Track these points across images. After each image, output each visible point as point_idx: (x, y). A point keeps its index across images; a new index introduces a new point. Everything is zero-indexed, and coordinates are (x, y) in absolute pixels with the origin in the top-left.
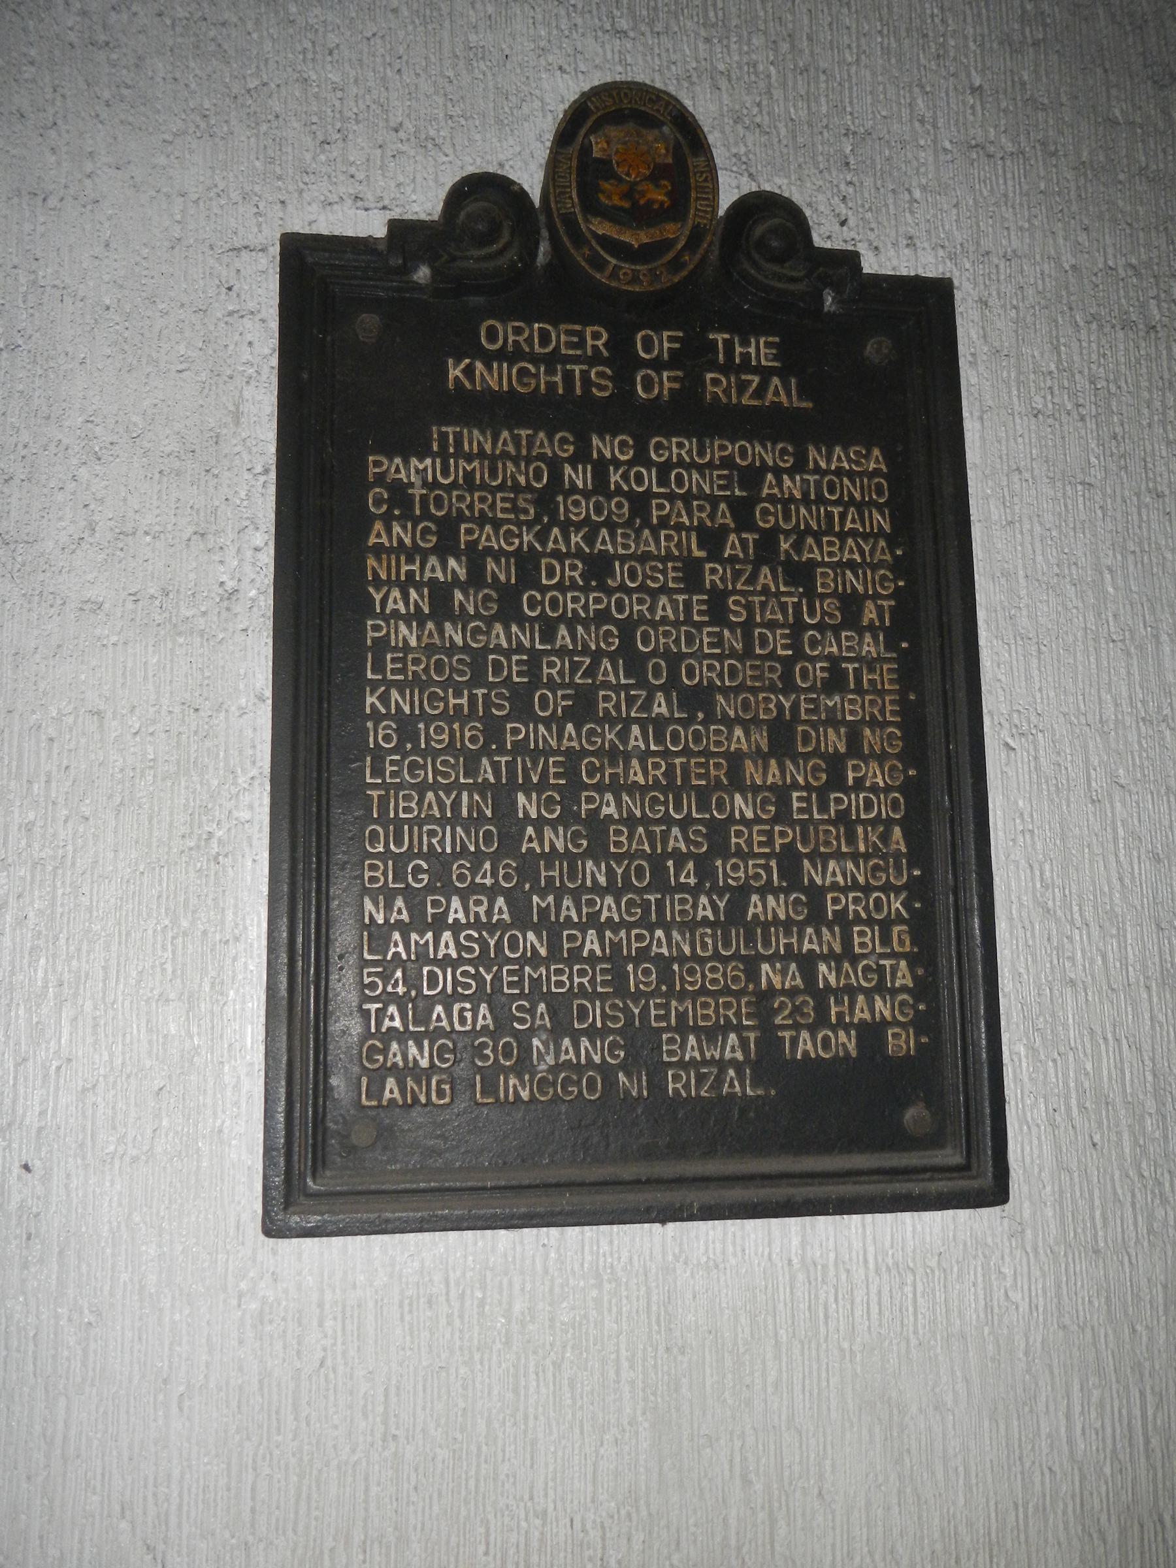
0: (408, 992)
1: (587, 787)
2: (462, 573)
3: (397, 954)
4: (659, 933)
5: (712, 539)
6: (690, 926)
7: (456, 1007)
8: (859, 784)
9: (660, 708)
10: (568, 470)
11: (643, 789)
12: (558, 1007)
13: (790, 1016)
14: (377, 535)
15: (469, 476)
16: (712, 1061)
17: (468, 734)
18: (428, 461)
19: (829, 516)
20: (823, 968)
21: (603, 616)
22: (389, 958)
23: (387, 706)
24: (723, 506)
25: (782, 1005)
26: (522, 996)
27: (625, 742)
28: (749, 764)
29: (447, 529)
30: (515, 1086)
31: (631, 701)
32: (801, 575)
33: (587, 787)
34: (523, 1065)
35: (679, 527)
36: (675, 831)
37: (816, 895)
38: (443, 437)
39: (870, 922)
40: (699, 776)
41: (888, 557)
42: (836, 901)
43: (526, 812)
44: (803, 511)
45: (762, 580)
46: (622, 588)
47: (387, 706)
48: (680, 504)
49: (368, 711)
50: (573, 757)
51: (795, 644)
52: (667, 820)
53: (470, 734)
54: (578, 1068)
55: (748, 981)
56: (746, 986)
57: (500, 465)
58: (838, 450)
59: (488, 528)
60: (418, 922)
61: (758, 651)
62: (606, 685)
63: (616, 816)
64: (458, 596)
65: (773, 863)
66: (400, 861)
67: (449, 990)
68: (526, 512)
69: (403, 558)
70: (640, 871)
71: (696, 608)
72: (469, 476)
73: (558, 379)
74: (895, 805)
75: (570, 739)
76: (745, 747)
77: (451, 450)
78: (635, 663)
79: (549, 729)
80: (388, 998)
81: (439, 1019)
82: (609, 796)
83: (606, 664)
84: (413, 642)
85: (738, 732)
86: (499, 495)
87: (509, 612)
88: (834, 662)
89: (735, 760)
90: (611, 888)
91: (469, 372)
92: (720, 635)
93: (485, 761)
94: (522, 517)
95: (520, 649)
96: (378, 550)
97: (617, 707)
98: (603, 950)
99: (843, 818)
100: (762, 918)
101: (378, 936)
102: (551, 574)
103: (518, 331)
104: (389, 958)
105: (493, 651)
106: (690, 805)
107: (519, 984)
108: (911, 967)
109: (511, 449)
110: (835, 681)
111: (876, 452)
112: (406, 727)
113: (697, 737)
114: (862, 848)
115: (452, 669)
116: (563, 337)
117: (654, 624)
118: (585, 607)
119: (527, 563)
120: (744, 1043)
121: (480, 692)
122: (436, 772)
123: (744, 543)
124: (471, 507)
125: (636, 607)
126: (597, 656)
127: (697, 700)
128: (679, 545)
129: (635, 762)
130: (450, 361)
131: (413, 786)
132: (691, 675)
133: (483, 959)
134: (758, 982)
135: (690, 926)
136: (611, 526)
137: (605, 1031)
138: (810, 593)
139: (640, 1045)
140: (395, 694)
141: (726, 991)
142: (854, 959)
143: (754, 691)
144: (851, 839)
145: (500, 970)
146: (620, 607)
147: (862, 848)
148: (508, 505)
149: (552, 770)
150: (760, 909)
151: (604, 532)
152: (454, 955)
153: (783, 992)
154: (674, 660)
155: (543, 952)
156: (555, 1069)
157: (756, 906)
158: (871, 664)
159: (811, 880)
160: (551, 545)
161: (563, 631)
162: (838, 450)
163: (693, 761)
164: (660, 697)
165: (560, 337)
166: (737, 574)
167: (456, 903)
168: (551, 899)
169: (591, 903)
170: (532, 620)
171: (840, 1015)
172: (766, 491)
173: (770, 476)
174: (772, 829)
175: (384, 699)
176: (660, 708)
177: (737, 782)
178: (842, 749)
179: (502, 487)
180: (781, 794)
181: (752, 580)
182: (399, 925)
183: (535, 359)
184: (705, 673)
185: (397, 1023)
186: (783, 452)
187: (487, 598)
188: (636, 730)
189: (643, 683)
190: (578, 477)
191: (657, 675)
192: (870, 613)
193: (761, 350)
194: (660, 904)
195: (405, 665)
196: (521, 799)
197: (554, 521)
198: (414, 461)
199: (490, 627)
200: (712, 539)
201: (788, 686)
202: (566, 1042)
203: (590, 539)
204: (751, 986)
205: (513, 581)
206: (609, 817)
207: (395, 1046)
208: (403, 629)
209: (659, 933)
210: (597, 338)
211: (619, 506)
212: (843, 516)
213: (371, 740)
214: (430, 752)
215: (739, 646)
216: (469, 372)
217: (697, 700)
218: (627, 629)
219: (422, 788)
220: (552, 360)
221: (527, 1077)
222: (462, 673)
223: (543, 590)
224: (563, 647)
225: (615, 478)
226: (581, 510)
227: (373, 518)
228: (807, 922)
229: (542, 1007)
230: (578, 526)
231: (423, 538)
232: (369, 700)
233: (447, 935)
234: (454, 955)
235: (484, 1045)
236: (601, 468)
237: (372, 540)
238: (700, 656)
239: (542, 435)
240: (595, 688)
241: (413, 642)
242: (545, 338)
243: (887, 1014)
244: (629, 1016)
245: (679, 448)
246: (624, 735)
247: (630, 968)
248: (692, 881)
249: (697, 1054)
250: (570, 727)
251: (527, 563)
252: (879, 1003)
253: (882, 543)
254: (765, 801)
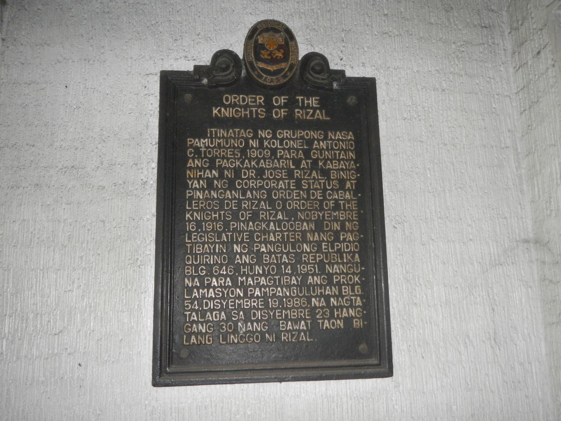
0: (199, 308)
2: (217, 175)
4: (279, 289)
5: (297, 163)
7: (214, 313)
8: (344, 240)
9: (280, 216)
10: (251, 141)
11: (274, 243)
12: (247, 312)
13: (322, 315)
14: (190, 164)
17: (218, 226)
18: (206, 140)
19: (335, 154)
20: (332, 300)
21: (262, 187)
23: (193, 217)
24: (300, 152)
25: (319, 312)
26: (235, 309)
27: (269, 228)
29: (212, 161)
32: (326, 173)
33: (256, 242)
34: (235, 331)
35: (286, 159)
36: (285, 256)
37: (330, 276)
38: (211, 132)
39: (348, 285)
40: (292, 238)
41: (354, 167)
44: (326, 152)
45: (313, 175)
46: (268, 178)
47: (193, 217)
48: (286, 151)
49: (187, 219)
50: (252, 233)
53: (219, 226)
58: (338, 133)
59: (225, 161)
60: (202, 286)
61: (312, 198)
62: (263, 210)
65: (316, 266)
66: (197, 267)
67: (212, 307)
68: (237, 155)
69: (198, 171)
71: (292, 184)
73: (248, 113)
75: (251, 227)
79: (244, 224)
80: (192, 310)
82: (263, 245)
83: (263, 203)
85: (305, 224)
86: (229, 150)
87: (231, 186)
88: (336, 201)
89: (304, 233)
90: (264, 275)
91: (220, 111)
92: (299, 193)
93: (224, 234)
95: (235, 198)
96: (190, 168)
97: (266, 216)
98: (261, 294)
99: (339, 251)
101: (190, 291)
102: (245, 174)
103: (235, 98)
105: (226, 199)
106: (289, 248)
107: (234, 305)
108: (361, 299)
109: (233, 135)
110: (337, 207)
111: (351, 133)
112: (199, 224)
114: (345, 261)
115: (213, 205)
116: (250, 100)
118: (256, 185)
120: (306, 324)
121: (222, 212)
123: (307, 163)
124: (220, 154)
126: (260, 200)
127: (292, 214)
128: (286, 164)
129: (272, 234)
130: (214, 108)
131: (201, 243)
132: (290, 206)
133: (223, 298)
135: (289, 286)
138: (329, 179)
140: (195, 214)
141: (301, 307)
142: (343, 297)
143: (310, 211)
144: (342, 258)
146: (267, 185)
147: (345, 261)
149: (245, 237)
150: (312, 281)
151: (262, 161)
152: (214, 296)
153: (319, 307)
154: (284, 201)
155: (242, 295)
159: (329, 271)
160: (245, 165)
161: (249, 193)
162: (338, 133)
163: (290, 234)
164: (280, 213)
165: (249, 99)
167: (214, 280)
168: (244, 278)
169: (257, 279)
171: (338, 315)
172: (314, 147)
173: (316, 142)
174: (316, 255)
175: (192, 215)
176: (280, 216)
177: (304, 240)
178: (339, 229)
179: (230, 147)
180: (319, 244)
181: (310, 175)
182: (196, 287)
183: (241, 107)
184: (294, 205)
185: (196, 318)
186: (320, 134)
188: (272, 224)
190: (254, 143)
191: (279, 206)
192: (348, 185)
193: (313, 101)
194: (280, 279)
196: (235, 246)
197: (246, 158)
198: (202, 140)
200: (297, 163)
201: (322, 209)
202: (249, 324)
203: (258, 163)
207: (194, 325)
208: (198, 193)
209: (279, 289)
210: (260, 99)
211: (267, 152)
212: (340, 154)
215: (305, 196)
216: (220, 111)
217: (292, 214)
219: (204, 243)
220: (246, 107)
222: (216, 207)
223: (243, 180)
224: (249, 198)
225: (266, 143)
226: (255, 154)
229: (241, 313)
230: (254, 159)
231: (205, 164)
232: (187, 216)
233: (211, 290)
234: (214, 296)
235: (223, 325)
237: (189, 165)
238: (293, 200)
239: (242, 130)
240: (259, 210)
241: (201, 197)
242: (244, 100)
243: (353, 314)
245: (286, 133)
246: (268, 225)
247: (270, 300)
248: (290, 272)
250: (251, 223)
251: (237, 172)
252: (350, 311)
253: (352, 162)
254: (314, 246)
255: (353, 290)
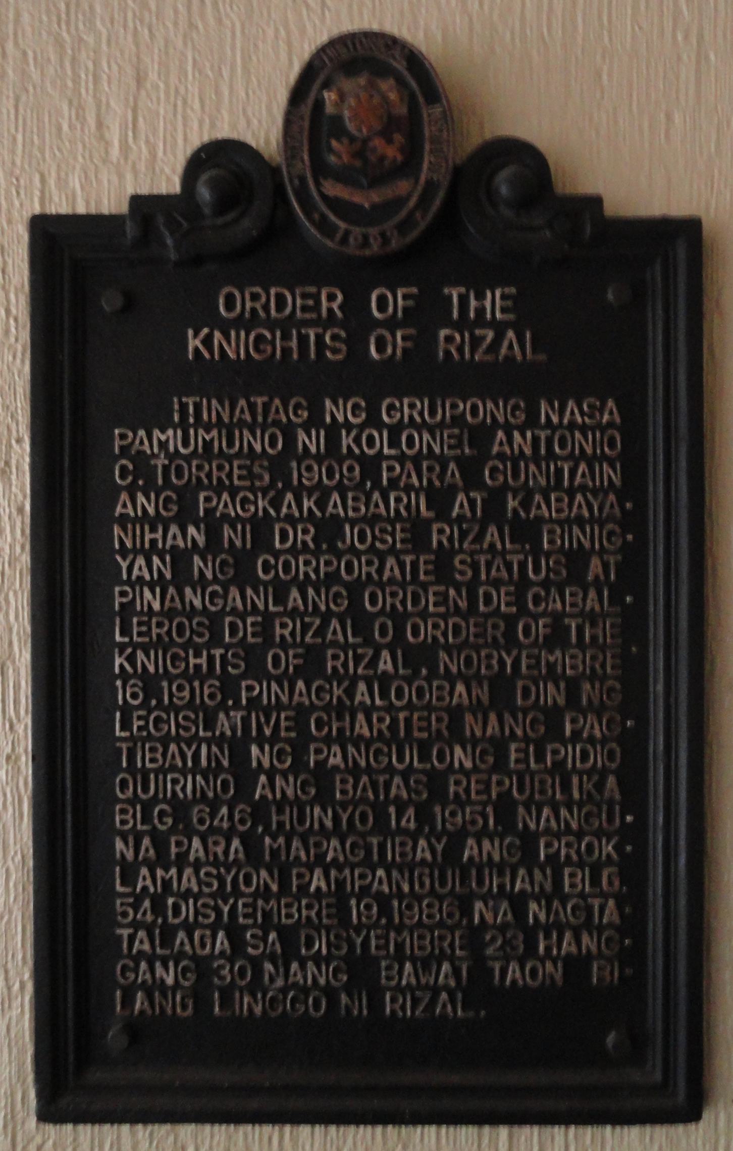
1: (315, 739)
2: (201, 540)
3: (145, 888)
4: (380, 873)
5: (440, 500)
6: (409, 867)
9: (385, 664)
10: (302, 436)
11: (368, 743)
12: (287, 936)
15: (208, 445)
16: (427, 987)
17: (206, 692)
18: (170, 432)
20: (533, 906)
21: (333, 578)
22: (138, 890)
23: (133, 664)
25: (494, 939)
27: (351, 697)
28: (468, 718)
30: (249, 1004)
31: (357, 659)
32: (526, 532)
33: (315, 739)
34: (256, 986)
35: (408, 489)
36: (397, 780)
37: (529, 840)
38: (183, 407)
39: (581, 865)
42: (548, 845)
43: (259, 763)
45: (488, 538)
46: (352, 549)
47: (133, 664)
48: (409, 466)
49: (117, 670)
50: (301, 714)
51: (519, 599)
52: (390, 770)
53: (207, 691)
54: (305, 991)
55: (462, 916)
56: (461, 920)
57: (237, 433)
59: (225, 496)
60: (162, 859)
61: (482, 608)
62: (334, 644)
63: (342, 766)
64: (197, 561)
65: (489, 810)
66: (147, 808)
67: (191, 919)
68: (261, 478)
70: (363, 818)
71: (422, 568)
72: (208, 445)
74: (611, 755)
76: (466, 701)
77: (191, 420)
78: (361, 622)
79: (281, 687)
81: (182, 944)
82: (336, 748)
84: (156, 606)
85: (460, 688)
86: (236, 464)
87: (243, 576)
88: (557, 619)
89: (456, 714)
90: (337, 831)
92: (446, 595)
94: (258, 484)
95: (255, 610)
97: (345, 665)
100: (477, 859)
104: (138, 890)
106: (412, 757)
109: (248, 417)
110: (557, 637)
112: (150, 685)
113: (420, 692)
114: (576, 795)
115: (192, 631)
117: (381, 585)
118: (317, 570)
119: (260, 528)
120: (456, 971)
121: (218, 652)
122: (178, 725)
123: (472, 503)
124: (209, 476)
125: (362, 568)
126: (326, 618)
127: (419, 658)
128: (408, 507)
129: (361, 717)
131: (159, 740)
132: (416, 633)
133: (221, 893)
134: (471, 919)
135: (409, 867)
136: (342, 490)
137: (328, 959)
138: (537, 551)
139: (361, 971)
140: (140, 655)
141: (441, 924)
143: (477, 648)
144: (566, 787)
145: (236, 903)
146: (349, 568)
147: (576, 795)
148: (244, 472)
149: (283, 724)
150: (476, 851)
151: (335, 497)
152: (196, 889)
153: (494, 926)
154: (399, 619)
155: (274, 888)
156: (284, 991)
157: (472, 848)
158: (593, 618)
159: (526, 826)
160: (284, 510)
161: (295, 593)
164: (385, 654)
166: (463, 535)
167: (196, 843)
168: (281, 840)
169: (317, 845)
170: (266, 584)
174: (490, 778)
175: (131, 659)
176: (385, 664)
177: (456, 734)
178: (561, 701)
180: (499, 746)
181: (479, 538)
182: (146, 862)
184: (427, 631)
185: (146, 947)
187: (223, 563)
188: (362, 687)
189: (368, 641)
190: (310, 441)
194: (382, 847)
195: (150, 629)
196: (254, 750)
197: (288, 486)
198: (156, 433)
199: (226, 592)
200: (440, 500)
201: (511, 640)
202: (294, 966)
203: (321, 504)
204: (464, 922)
205: (249, 546)
206: (336, 768)
208: (147, 594)
211: (351, 469)
213: (120, 697)
214: (173, 707)
215: (463, 604)
217: (419, 658)
218: (355, 589)
219: (165, 741)
221: (259, 996)
222: (201, 635)
223: (277, 554)
224: (295, 609)
225: (346, 441)
226: (318, 473)
227: (118, 489)
228: (521, 863)
229: (272, 936)
230: (310, 492)
231: (166, 508)
232: (118, 661)
233: (188, 872)
234: (196, 889)
236: (333, 431)
237: (119, 510)
239: (277, 402)
240: (324, 646)
241: (156, 606)
244: (351, 945)
246: (350, 692)
247: (353, 902)
248: (412, 825)
249: (413, 981)
250: (300, 685)
251: (260, 528)
254: (483, 753)
255: (595, 880)
